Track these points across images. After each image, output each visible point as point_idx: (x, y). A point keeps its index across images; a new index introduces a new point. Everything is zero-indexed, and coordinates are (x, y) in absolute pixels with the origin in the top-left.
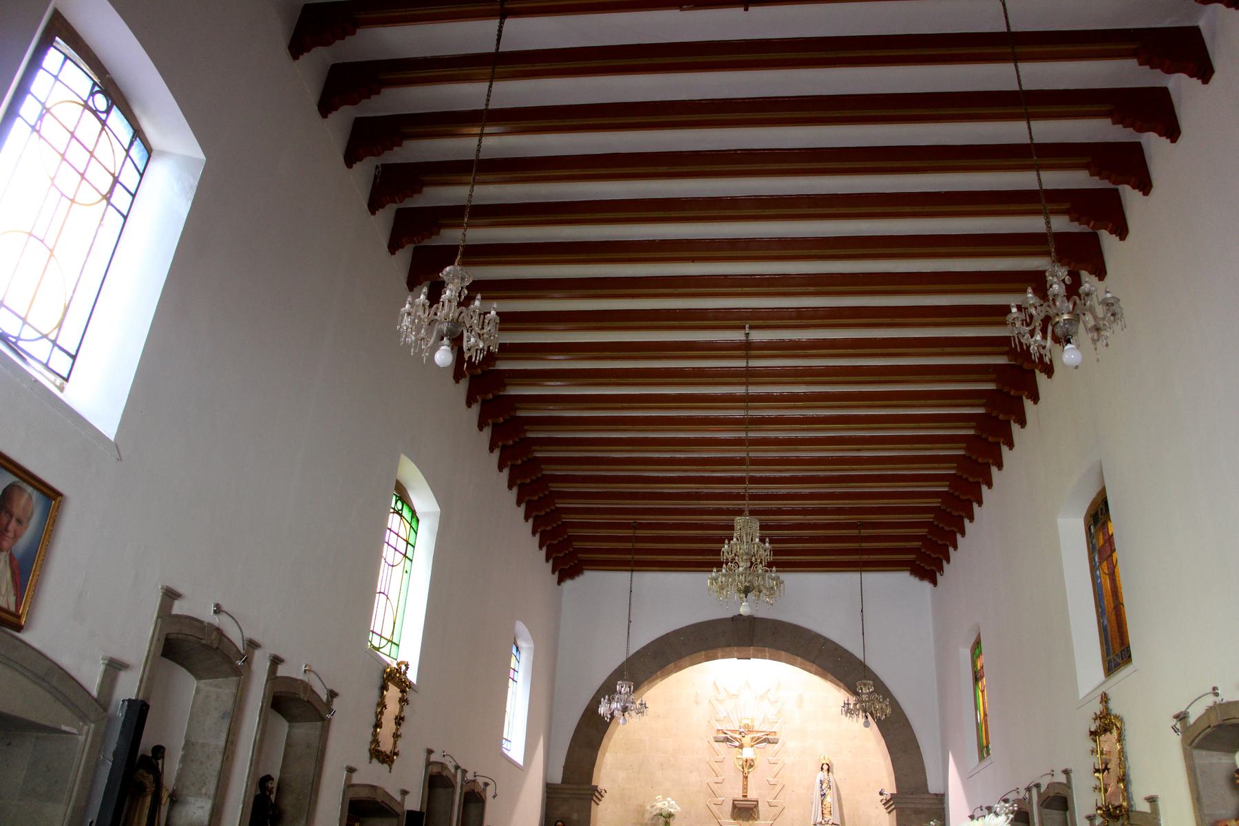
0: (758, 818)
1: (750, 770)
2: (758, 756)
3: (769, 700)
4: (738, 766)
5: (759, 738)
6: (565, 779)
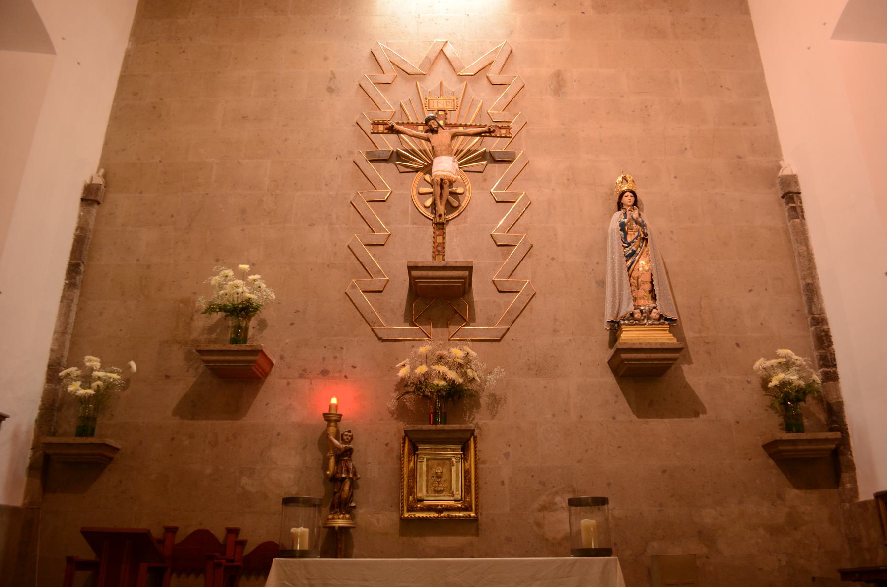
0: (472, 319)
1: (450, 216)
2: (469, 186)
4: (423, 210)
5: (469, 152)
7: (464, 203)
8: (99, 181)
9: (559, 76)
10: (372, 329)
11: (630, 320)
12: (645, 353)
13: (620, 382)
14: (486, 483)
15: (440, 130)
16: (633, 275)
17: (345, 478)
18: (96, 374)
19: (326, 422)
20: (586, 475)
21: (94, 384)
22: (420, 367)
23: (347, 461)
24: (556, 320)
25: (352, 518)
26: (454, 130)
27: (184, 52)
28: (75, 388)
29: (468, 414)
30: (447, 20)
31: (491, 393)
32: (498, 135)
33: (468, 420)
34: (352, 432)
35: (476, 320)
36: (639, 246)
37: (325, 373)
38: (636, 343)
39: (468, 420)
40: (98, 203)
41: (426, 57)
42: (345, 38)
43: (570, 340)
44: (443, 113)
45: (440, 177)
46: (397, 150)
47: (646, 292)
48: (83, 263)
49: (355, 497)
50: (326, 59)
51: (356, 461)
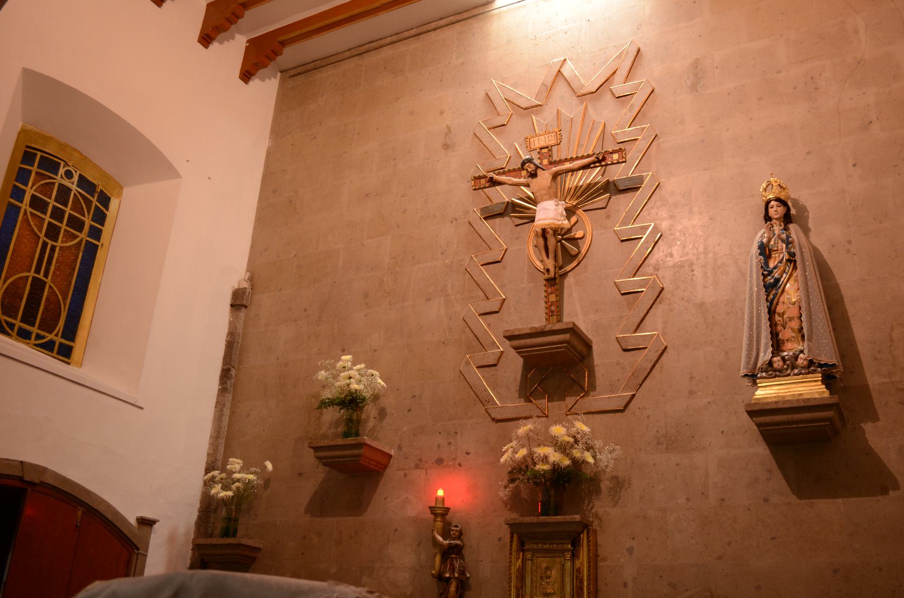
0: (593, 387)
1: (568, 268)
2: (589, 229)
5: (590, 186)
7: (584, 248)
8: (246, 285)
9: (697, 67)
10: (486, 411)
11: (770, 371)
12: (784, 414)
14: (606, 584)
15: (539, 172)
16: (777, 311)
17: (449, 579)
18: (237, 476)
19: (433, 516)
20: (728, 576)
21: (234, 487)
22: (521, 449)
23: (453, 558)
24: (691, 378)
26: (555, 169)
27: (315, 138)
29: (586, 502)
30: (566, 33)
31: (614, 475)
32: (609, 163)
33: (587, 509)
34: (460, 526)
35: (597, 388)
36: (784, 272)
37: (439, 461)
38: (771, 403)
39: (587, 509)
40: (246, 307)
41: (543, 84)
42: (459, 85)
43: (709, 403)
44: (546, 150)
45: (540, 227)
46: (512, 200)
47: (794, 332)
48: (234, 368)
50: (442, 113)
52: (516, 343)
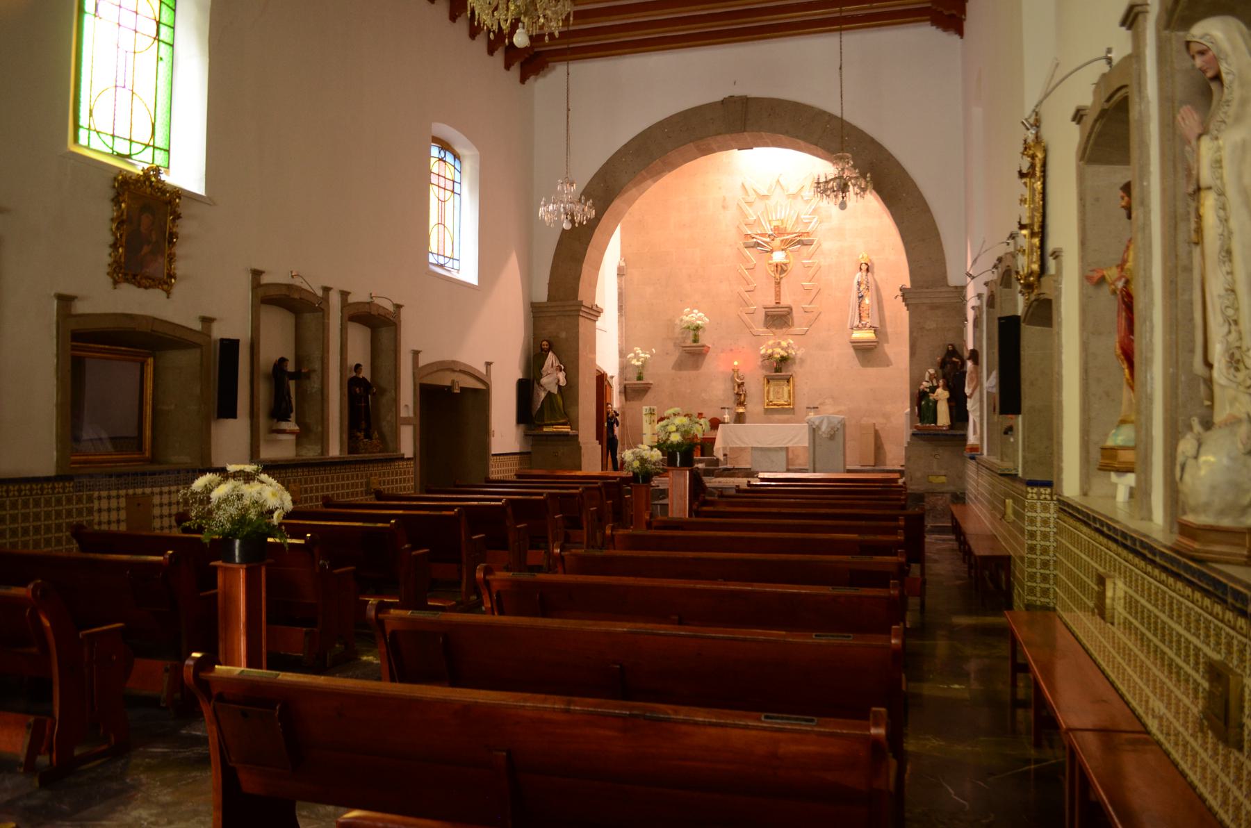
2: (792, 260)
3: (802, 198)
4: (770, 272)
5: (792, 241)
6: (551, 297)
8: (623, 264)
13: (856, 353)
17: (741, 395)
25: (745, 408)
28: (634, 362)
49: (746, 401)
50: (720, 188)
51: (746, 386)
52: (767, 310)
